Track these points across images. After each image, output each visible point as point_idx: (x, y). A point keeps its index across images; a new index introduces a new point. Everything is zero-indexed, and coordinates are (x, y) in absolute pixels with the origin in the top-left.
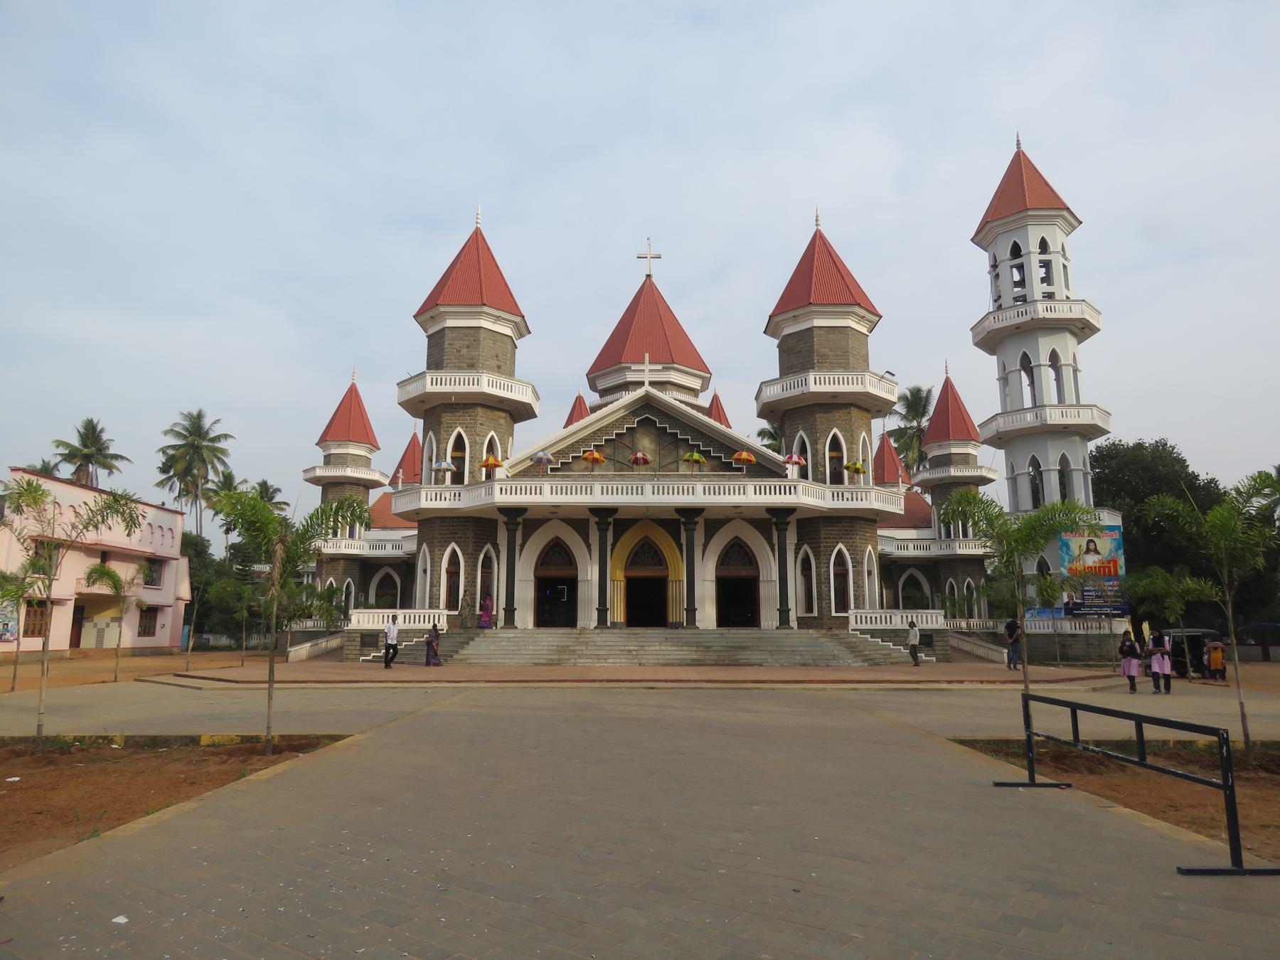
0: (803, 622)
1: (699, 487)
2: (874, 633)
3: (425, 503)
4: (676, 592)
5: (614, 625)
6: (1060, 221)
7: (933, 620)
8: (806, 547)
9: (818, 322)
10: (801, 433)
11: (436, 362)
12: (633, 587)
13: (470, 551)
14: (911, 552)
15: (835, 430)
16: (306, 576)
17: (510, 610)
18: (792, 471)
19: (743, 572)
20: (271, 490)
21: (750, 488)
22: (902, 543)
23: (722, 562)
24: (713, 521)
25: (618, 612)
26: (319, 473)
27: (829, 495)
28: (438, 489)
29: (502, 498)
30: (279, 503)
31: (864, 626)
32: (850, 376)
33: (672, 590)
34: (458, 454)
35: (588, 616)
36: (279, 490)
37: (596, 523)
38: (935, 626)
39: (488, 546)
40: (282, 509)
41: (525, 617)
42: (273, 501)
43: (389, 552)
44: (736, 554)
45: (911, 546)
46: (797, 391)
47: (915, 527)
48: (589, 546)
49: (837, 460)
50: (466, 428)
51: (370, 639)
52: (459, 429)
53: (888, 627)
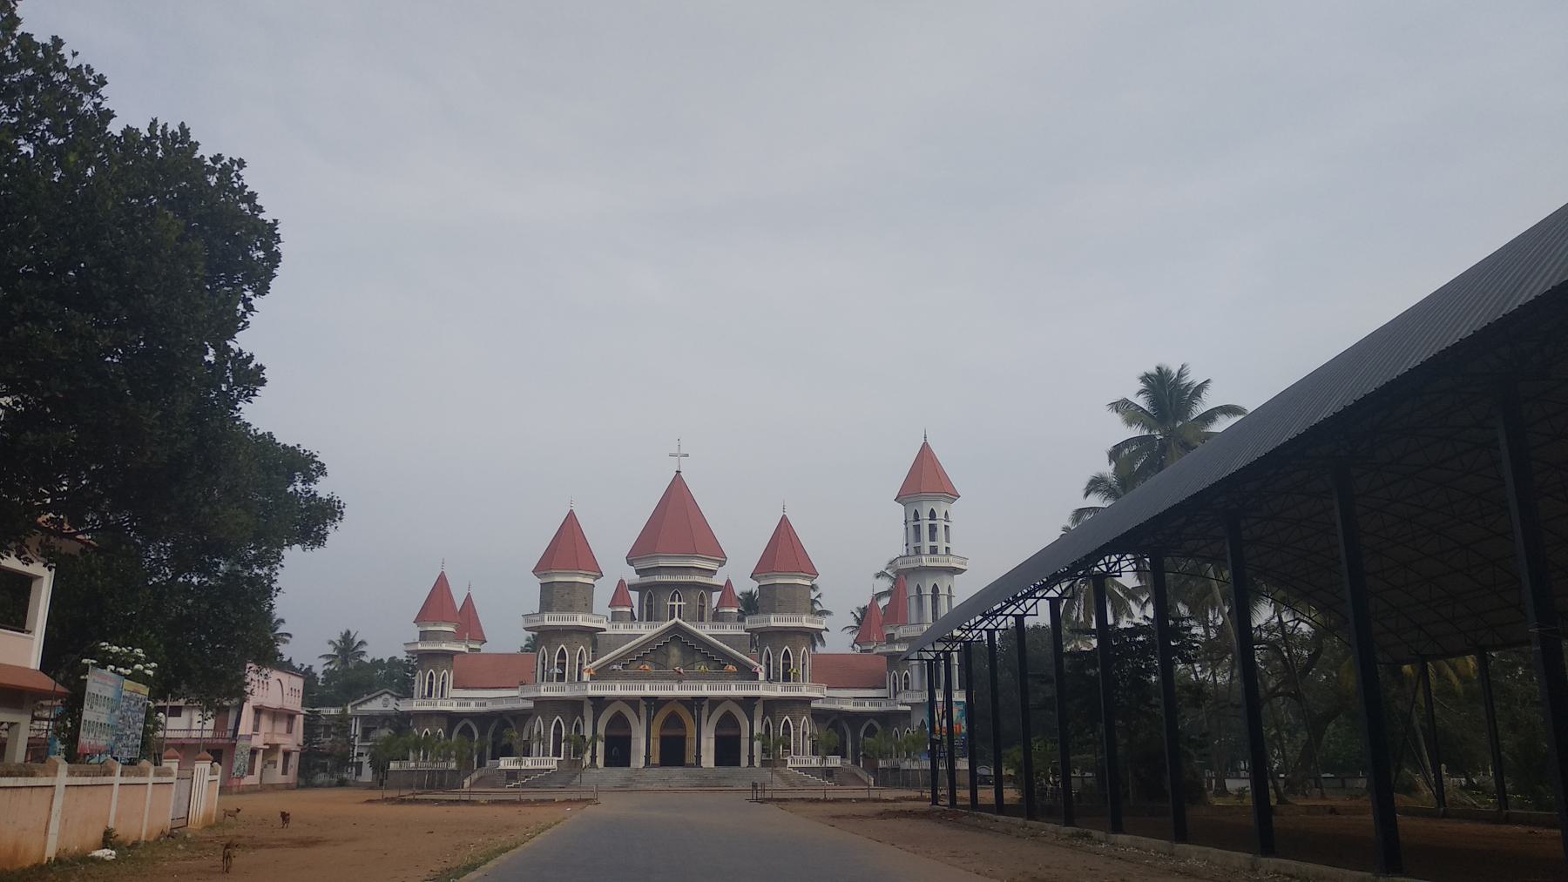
0: (763, 763)
1: (705, 686)
2: (800, 769)
3: (544, 694)
4: (690, 745)
5: (654, 766)
6: (943, 498)
7: (835, 761)
8: (767, 717)
9: (778, 581)
10: (768, 647)
11: (546, 606)
12: (664, 741)
13: (568, 721)
14: (867, 707)
15: (786, 647)
16: (354, 720)
17: (593, 757)
18: (762, 676)
19: (732, 733)
20: (275, 620)
21: (733, 687)
22: (861, 701)
23: (719, 726)
24: (715, 702)
25: (655, 759)
26: (420, 647)
27: (779, 688)
28: (550, 685)
29: (591, 693)
30: (282, 634)
31: (795, 766)
32: (793, 616)
33: (688, 743)
34: (562, 661)
35: (638, 760)
36: (283, 621)
37: (646, 706)
38: (835, 765)
39: (578, 717)
40: (285, 642)
41: (600, 761)
42: (277, 632)
43: (472, 707)
44: (728, 721)
45: (867, 704)
46: (764, 625)
47: (874, 688)
48: (639, 717)
49: (787, 666)
50: (566, 645)
51: (512, 775)
52: (562, 646)
53: (809, 765)
